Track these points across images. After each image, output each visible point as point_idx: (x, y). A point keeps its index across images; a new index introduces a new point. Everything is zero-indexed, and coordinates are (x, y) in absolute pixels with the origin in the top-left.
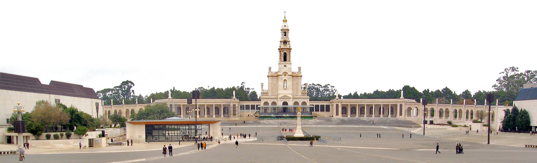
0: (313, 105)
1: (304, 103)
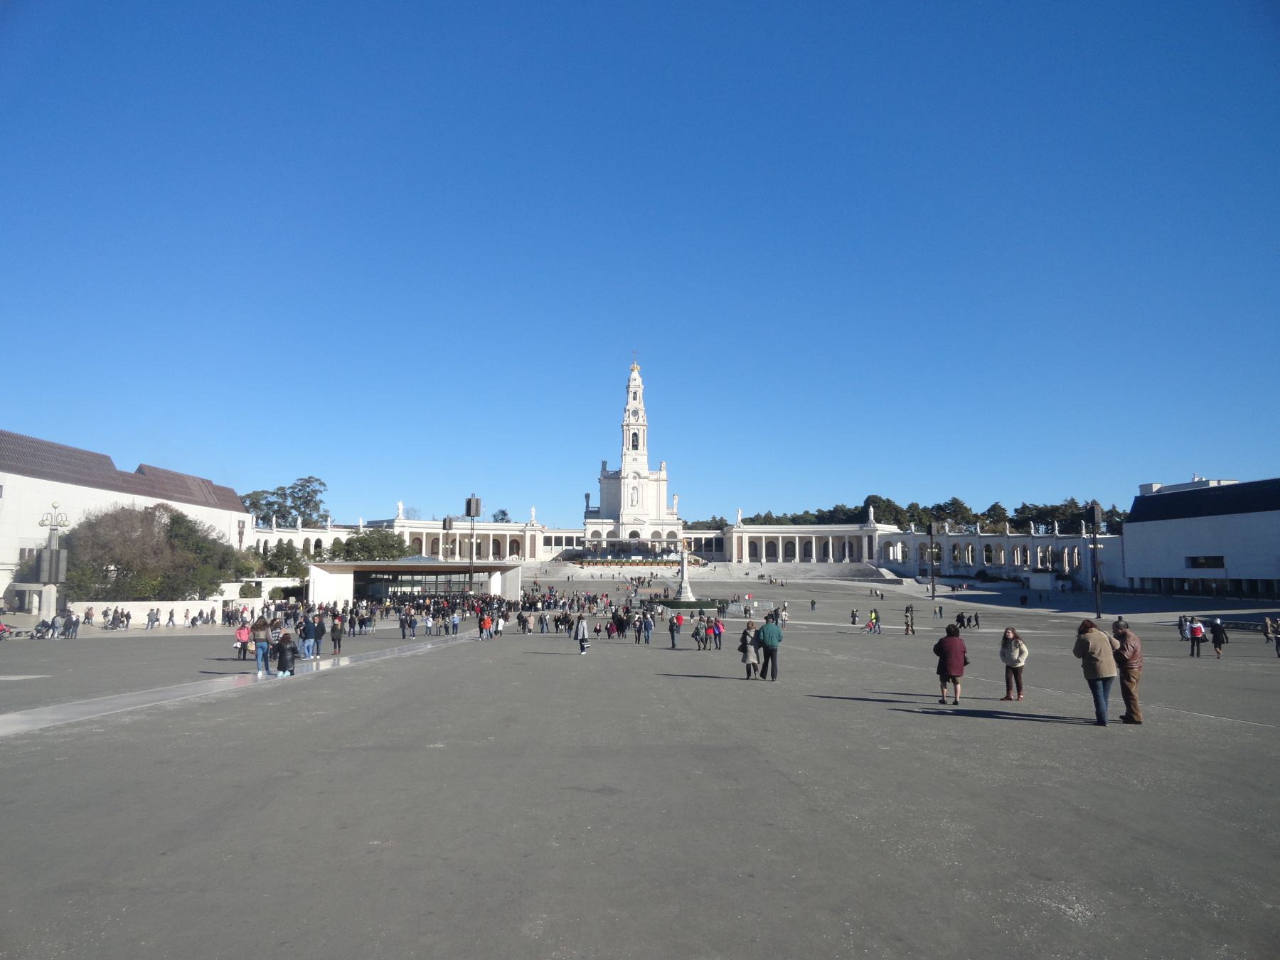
0: (691, 538)
1: (672, 535)
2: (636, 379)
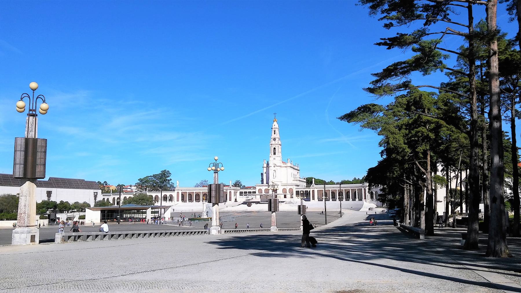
2: (276, 125)
